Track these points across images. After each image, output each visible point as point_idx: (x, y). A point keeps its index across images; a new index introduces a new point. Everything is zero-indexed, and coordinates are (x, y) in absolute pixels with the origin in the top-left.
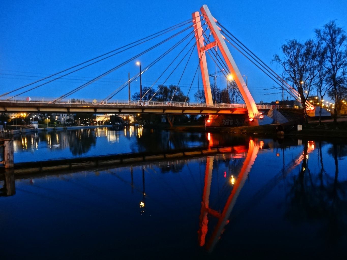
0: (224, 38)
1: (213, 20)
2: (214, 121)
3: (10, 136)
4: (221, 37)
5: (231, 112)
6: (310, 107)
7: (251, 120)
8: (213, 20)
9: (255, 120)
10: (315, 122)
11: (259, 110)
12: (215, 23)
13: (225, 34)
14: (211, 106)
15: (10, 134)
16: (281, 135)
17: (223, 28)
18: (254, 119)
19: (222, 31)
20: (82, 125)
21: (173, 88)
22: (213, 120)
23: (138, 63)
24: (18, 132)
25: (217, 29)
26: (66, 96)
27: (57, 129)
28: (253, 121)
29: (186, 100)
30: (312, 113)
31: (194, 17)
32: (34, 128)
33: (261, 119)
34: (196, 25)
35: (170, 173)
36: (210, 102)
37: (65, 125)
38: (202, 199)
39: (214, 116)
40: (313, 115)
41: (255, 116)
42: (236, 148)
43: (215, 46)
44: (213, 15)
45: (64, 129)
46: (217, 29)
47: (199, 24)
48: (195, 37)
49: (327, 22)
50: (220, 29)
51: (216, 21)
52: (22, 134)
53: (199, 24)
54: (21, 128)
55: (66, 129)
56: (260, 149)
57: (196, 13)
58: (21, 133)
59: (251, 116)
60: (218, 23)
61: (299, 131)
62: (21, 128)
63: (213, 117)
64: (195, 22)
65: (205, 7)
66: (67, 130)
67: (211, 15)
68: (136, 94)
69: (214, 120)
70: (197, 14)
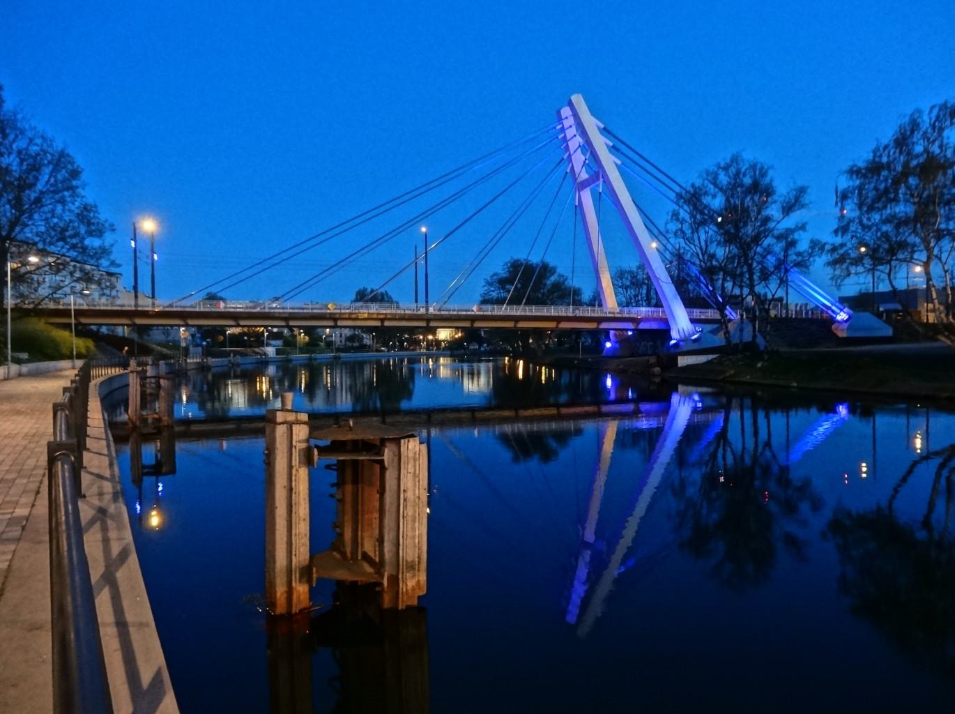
0: (619, 162)
1: (591, 124)
2: (617, 346)
3: (206, 369)
4: (609, 162)
5: (635, 324)
6: (842, 313)
7: (673, 342)
8: (591, 124)
9: (681, 343)
10: (839, 349)
11: (693, 321)
12: (598, 133)
13: (623, 153)
14: (610, 313)
15: (205, 365)
16: (654, 375)
17: (616, 141)
18: (679, 341)
19: (614, 150)
20: (382, 351)
21: (545, 270)
22: (616, 342)
23: (424, 230)
24: (225, 363)
25: (600, 143)
26: (286, 298)
27: (316, 359)
28: (676, 345)
29: (524, 301)
30: (843, 330)
31: (560, 119)
32: (265, 354)
33: (695, 341)
34: (565, 135)
35: (534, 464)
36: (611, 303)
37: (338, 350)
38: (582, 520)
39: (617, 333)
40: (842, 334)
41: (682, 335)
42: (645, 407)
43: (598, 183)
44: (593, 112)
45: (335, 358)
46: (600, 143)
47: (571, 132)
48: (563, 161)
49: (724, 157)
50: (611, 144)
51: (602, 126)
52: (233, 367)
53: (571, 132)
54: (232, 355)
55: (340, 358)
56: (695, 411)
57: (562, 111)
58: (231, 365)
59: (674, 334)
60: (605, 131)
61: (680, 368)
62: (232, 355)
63: (615, 335)
64: (563, 130)
65: (578, 99)
66: (340, 362)
67: (589, 113)
68: (495, 277)
69: (622, 341)
70: (566, 111)
